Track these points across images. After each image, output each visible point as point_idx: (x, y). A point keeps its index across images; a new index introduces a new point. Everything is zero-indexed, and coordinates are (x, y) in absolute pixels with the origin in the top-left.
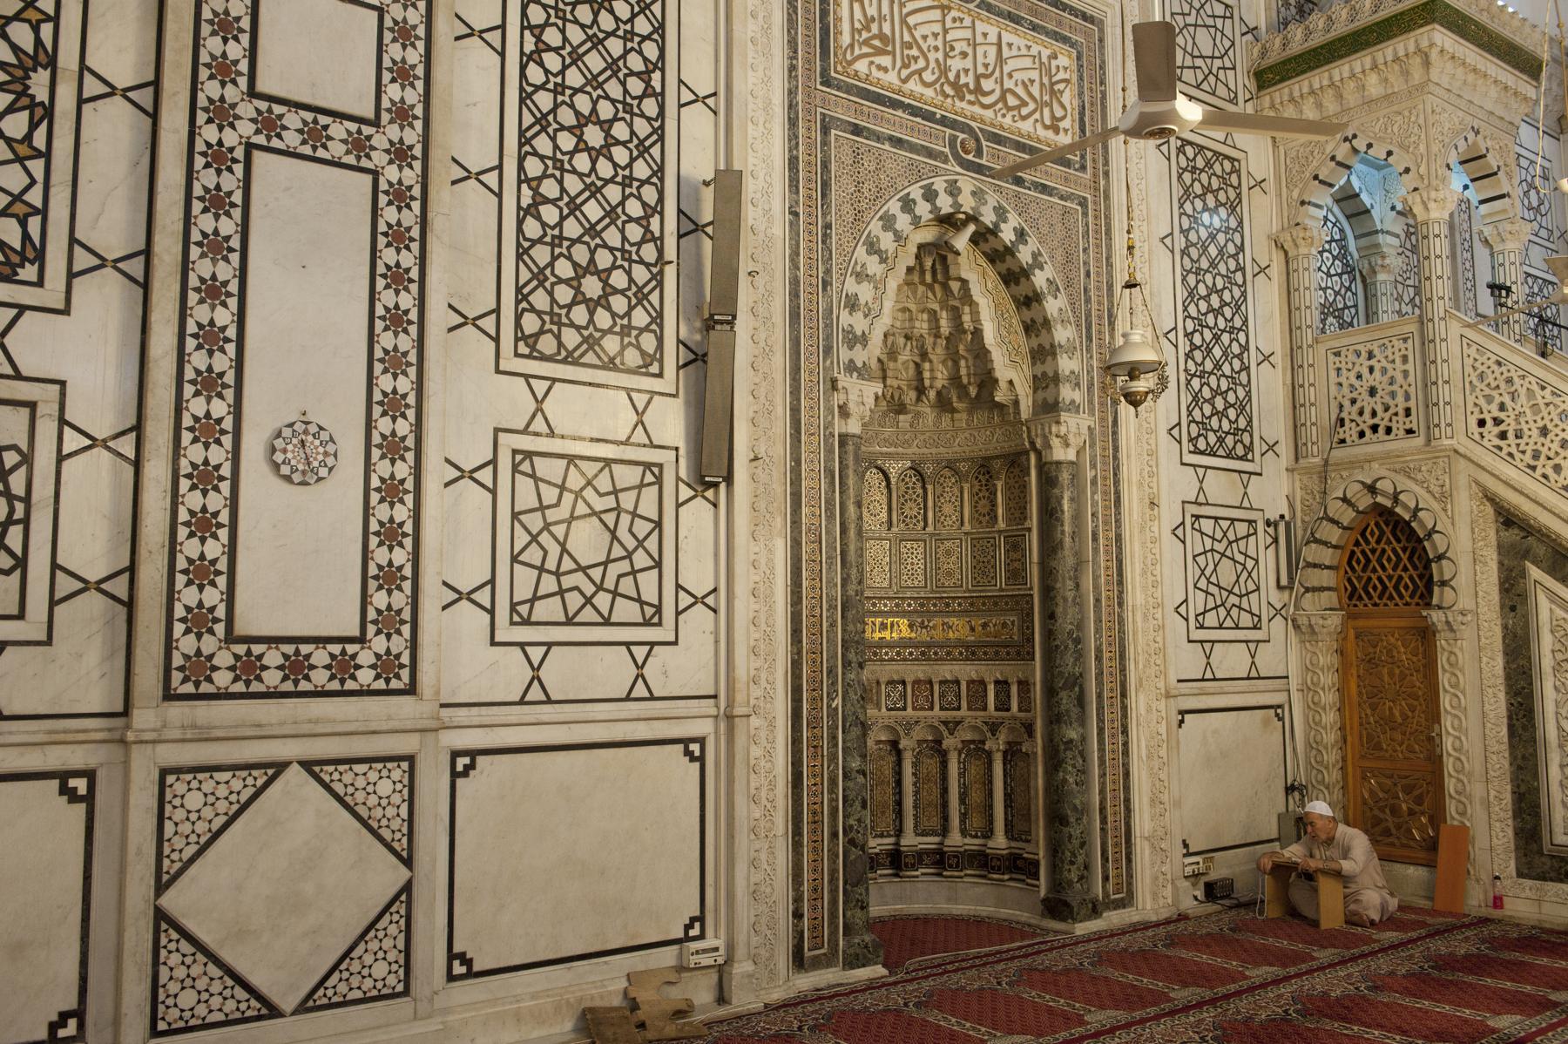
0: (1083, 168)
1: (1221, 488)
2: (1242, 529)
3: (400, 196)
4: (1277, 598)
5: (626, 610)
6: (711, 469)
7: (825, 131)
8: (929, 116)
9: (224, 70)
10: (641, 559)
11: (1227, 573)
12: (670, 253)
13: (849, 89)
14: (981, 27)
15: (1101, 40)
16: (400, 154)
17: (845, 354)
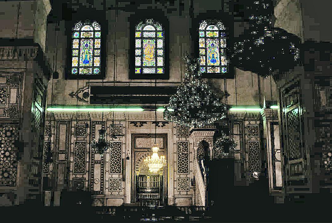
0: (164, 148)
1: (183, 176)
2: (186, 180)
3: (103, 164)
4: (191, 186)
5: (118, 189)
6: (124, 179)
7: (135, 152)
8: (145, 149)
9: (93, 160)
10: (119, 186)
11: (183, 184)
12: (121, 164)
13: (137, 148)
14: (151, 139)
15: (167, 136)
16: (102, 162)
17: (136, 169)
